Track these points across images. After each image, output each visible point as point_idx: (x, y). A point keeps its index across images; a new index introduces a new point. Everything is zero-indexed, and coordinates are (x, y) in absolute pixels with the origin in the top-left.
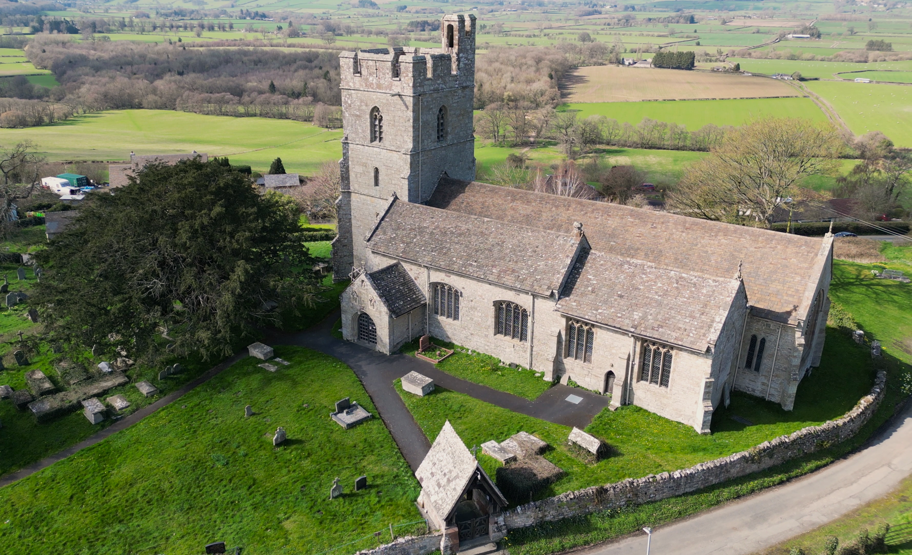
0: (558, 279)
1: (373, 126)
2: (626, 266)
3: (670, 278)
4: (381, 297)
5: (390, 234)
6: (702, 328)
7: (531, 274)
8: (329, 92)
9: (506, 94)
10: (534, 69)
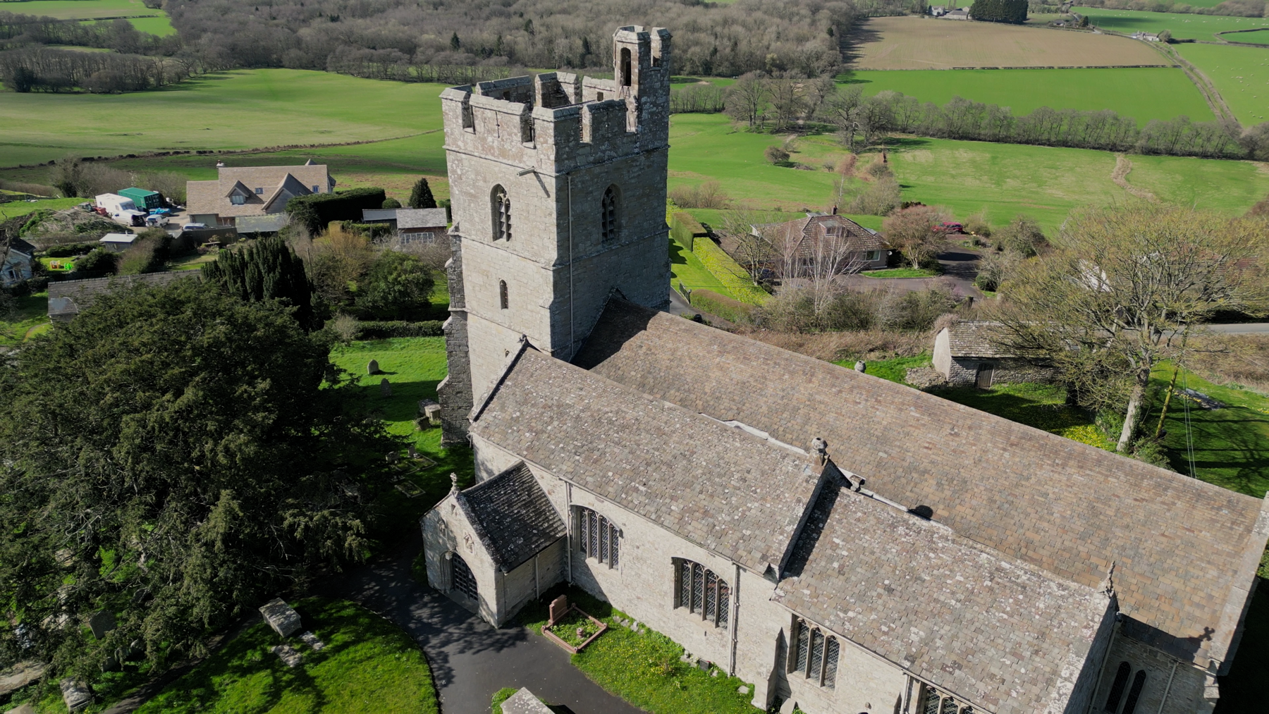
0: (780, 543)
1: (496, 214)
2: (901, 530)
3: (978, 567)
4: (481, 536)
5: (512, 411)
6: (1034, 682)
7: (735, 524)
8: (530, 49)
9: (769, 56)
10: (808, 20)
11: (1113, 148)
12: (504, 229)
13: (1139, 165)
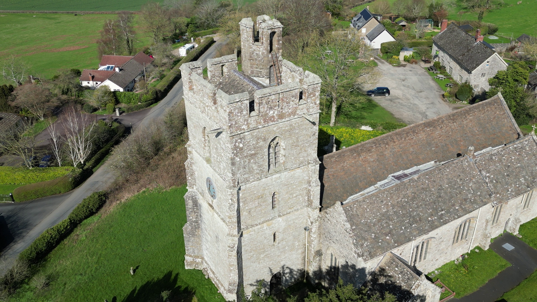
3: (513, 151)
12: (272, 160)
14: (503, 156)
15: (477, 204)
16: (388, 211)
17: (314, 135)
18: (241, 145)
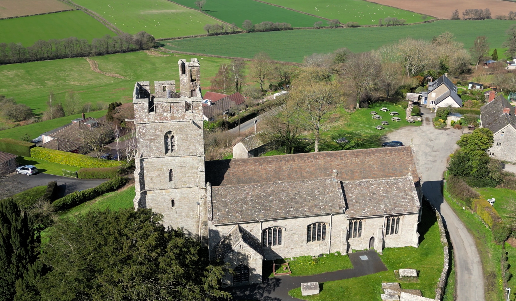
1: (166, 143)
2: (362, 184)
3: (384, 184)
6: (410, 202)
7: (326, 204)
11: (82, 55)
12: (170, 147)
13: (98, 60)
14: (372, 185)
15: (325, 211)
16: (246, 198)
17: (200, 135)
18: (144, 131)
